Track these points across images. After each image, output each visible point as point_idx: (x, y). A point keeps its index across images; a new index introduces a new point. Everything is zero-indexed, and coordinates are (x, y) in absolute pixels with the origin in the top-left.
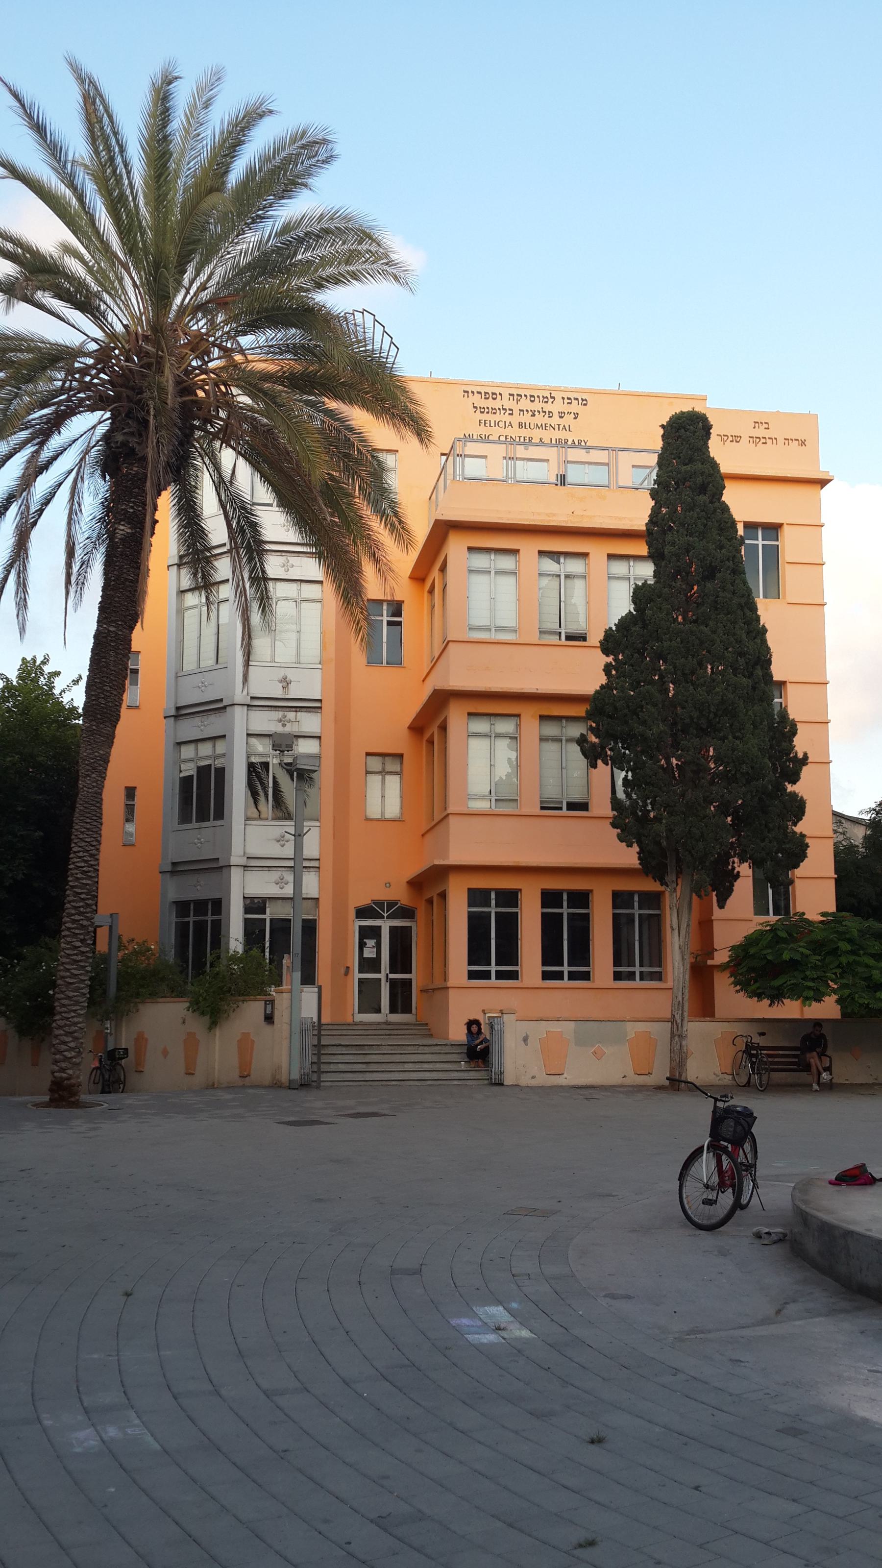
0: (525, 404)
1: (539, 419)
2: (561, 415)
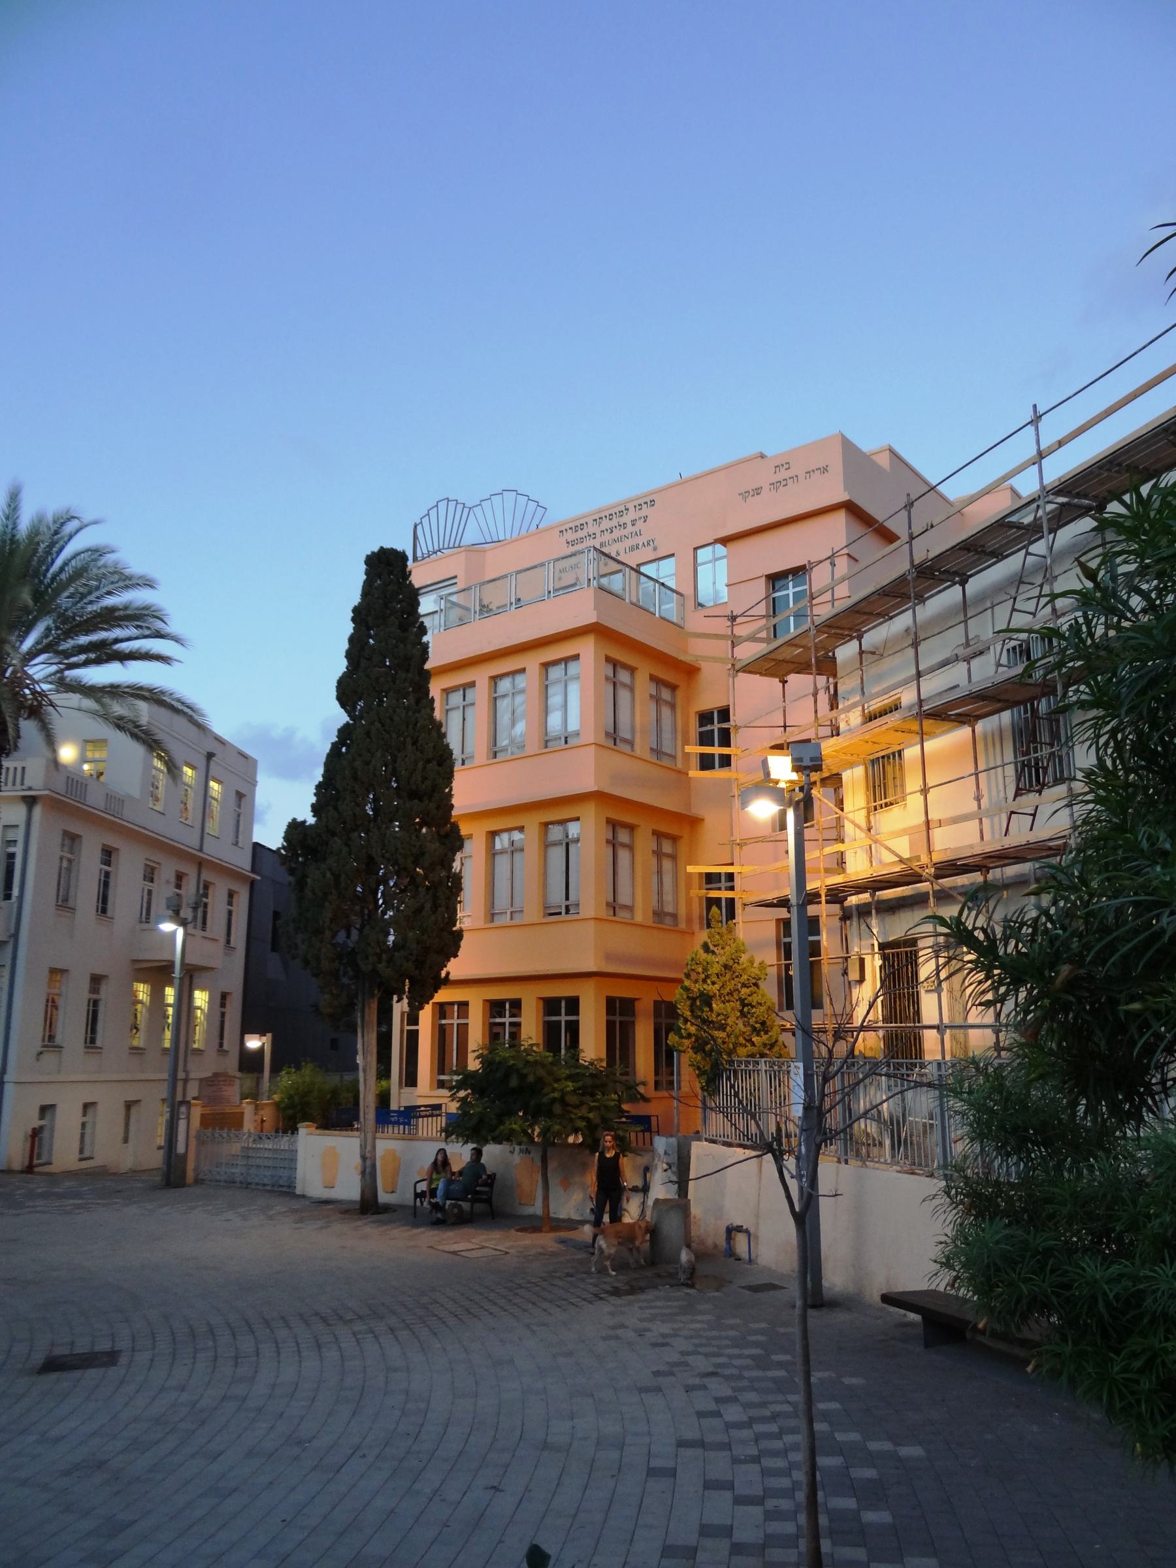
0: (606, 524)
1: (617, 533)
2: (633, 523)
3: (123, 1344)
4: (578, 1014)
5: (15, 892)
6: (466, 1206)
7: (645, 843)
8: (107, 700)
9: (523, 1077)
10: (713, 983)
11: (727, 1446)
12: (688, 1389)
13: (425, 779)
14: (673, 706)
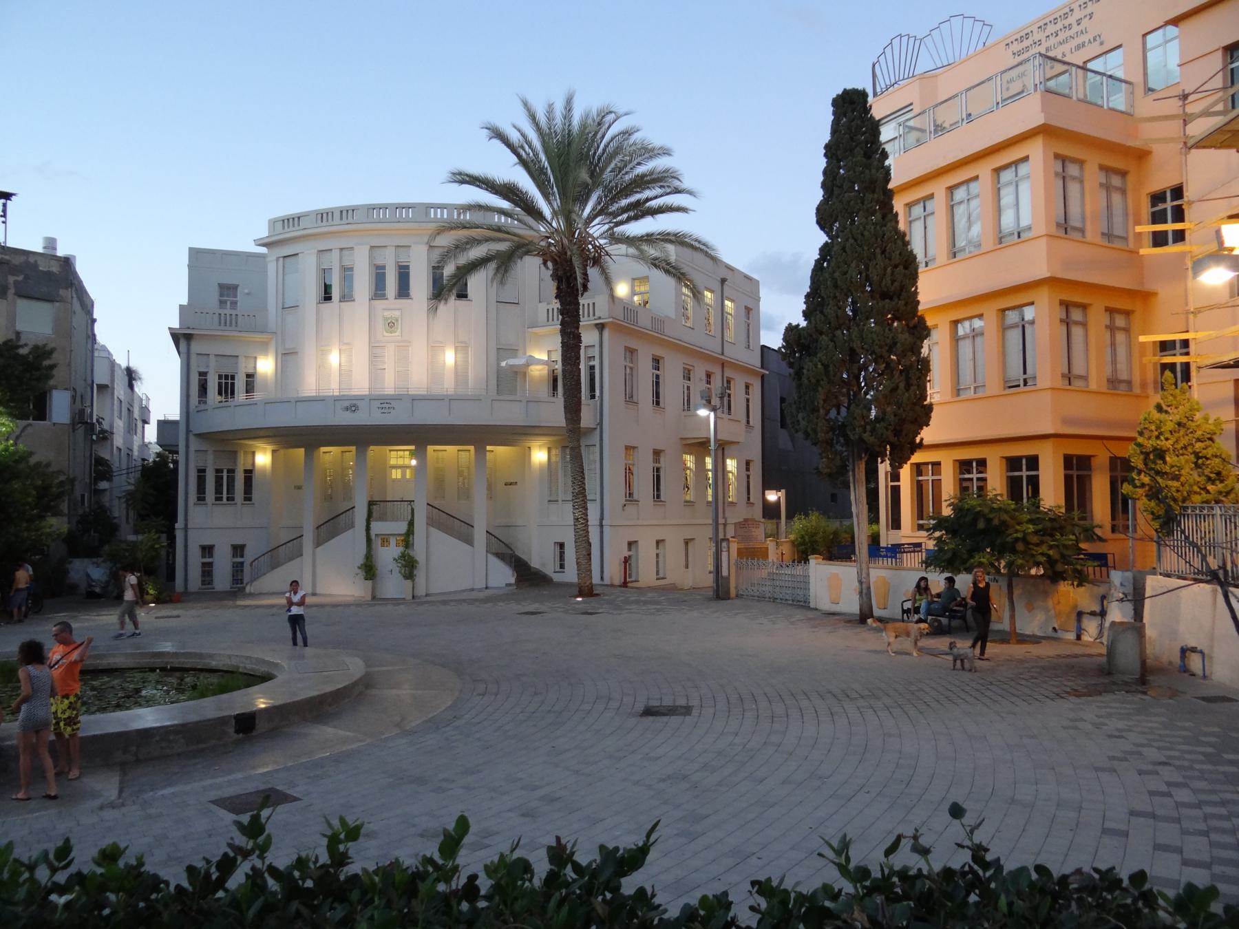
0: (1051, 29)
3: (694, 702)
4: (1037, 469)
5: (597, 393)
6: (944, 621)
7: (1097, 319)
8: (645, 247)
9: (989, 521)
10: (1167, 439)
11: (1178, 820)
12: (1140, 773)
13: (893, 281)
14: (1123, 192)
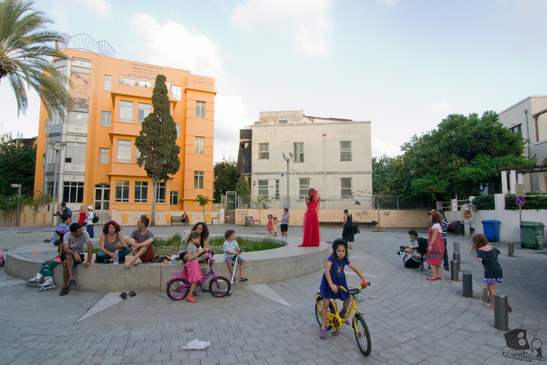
0: (146, 68)
1: (149, 72)
2: (155, 72)
